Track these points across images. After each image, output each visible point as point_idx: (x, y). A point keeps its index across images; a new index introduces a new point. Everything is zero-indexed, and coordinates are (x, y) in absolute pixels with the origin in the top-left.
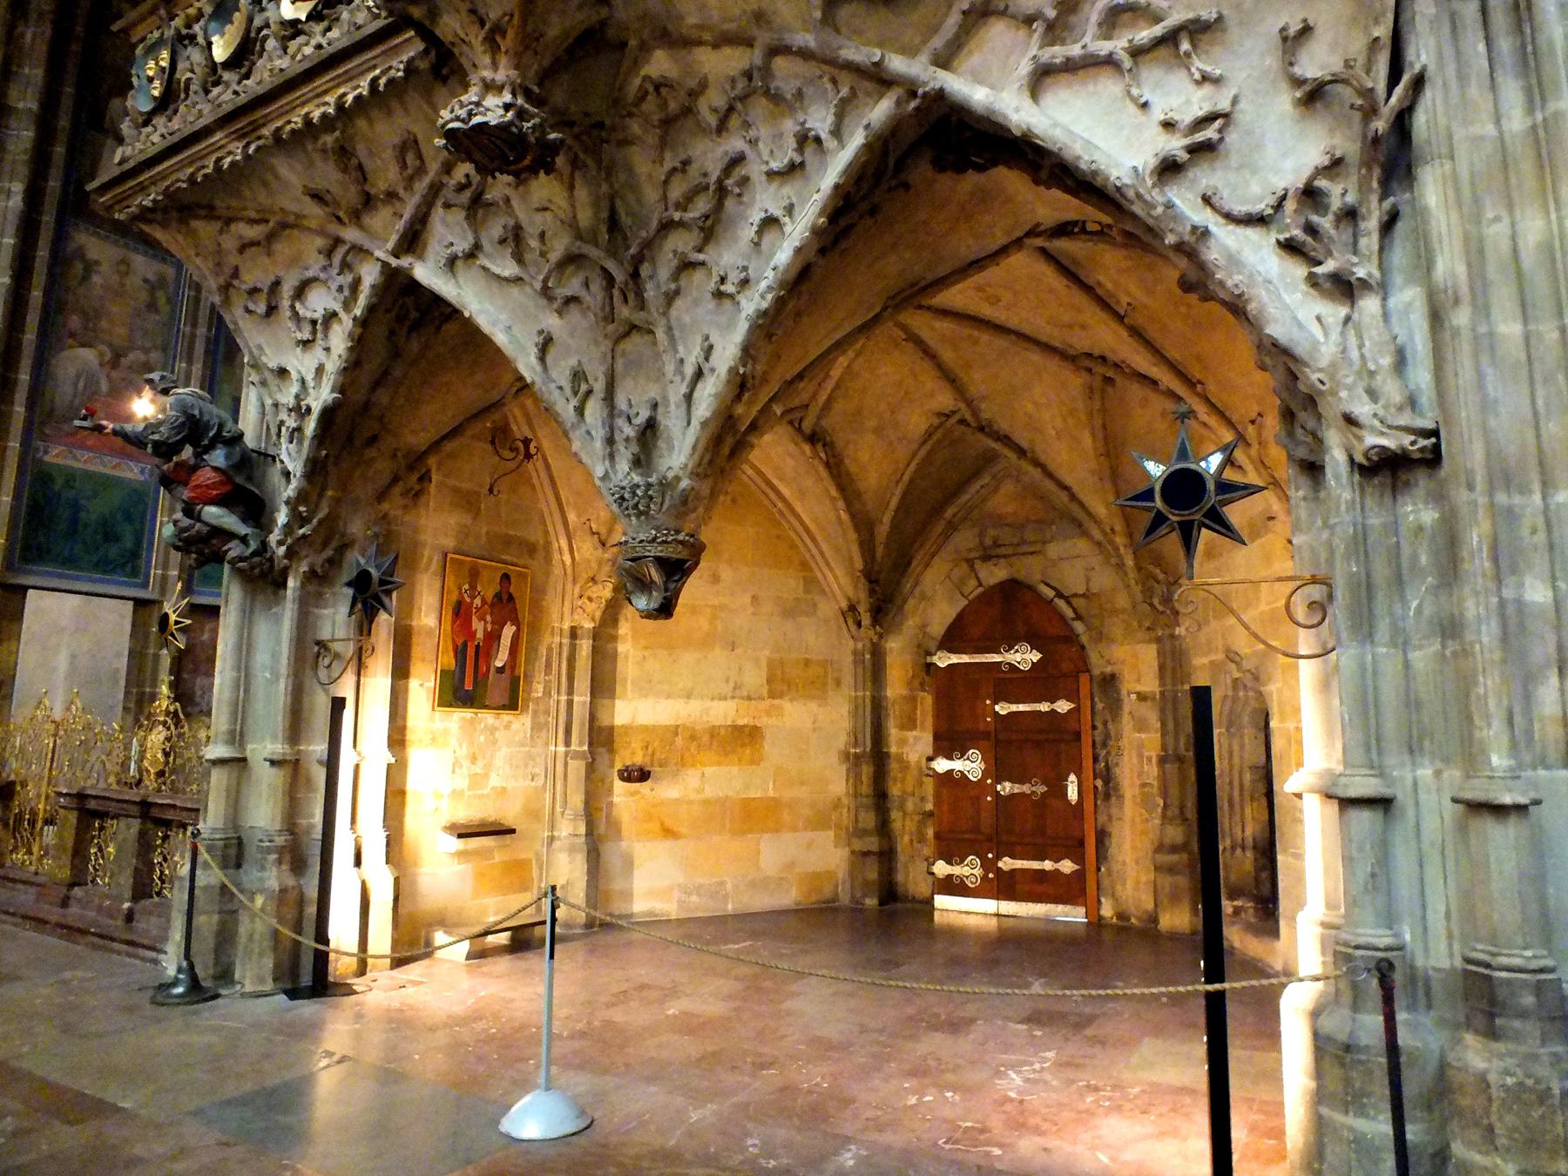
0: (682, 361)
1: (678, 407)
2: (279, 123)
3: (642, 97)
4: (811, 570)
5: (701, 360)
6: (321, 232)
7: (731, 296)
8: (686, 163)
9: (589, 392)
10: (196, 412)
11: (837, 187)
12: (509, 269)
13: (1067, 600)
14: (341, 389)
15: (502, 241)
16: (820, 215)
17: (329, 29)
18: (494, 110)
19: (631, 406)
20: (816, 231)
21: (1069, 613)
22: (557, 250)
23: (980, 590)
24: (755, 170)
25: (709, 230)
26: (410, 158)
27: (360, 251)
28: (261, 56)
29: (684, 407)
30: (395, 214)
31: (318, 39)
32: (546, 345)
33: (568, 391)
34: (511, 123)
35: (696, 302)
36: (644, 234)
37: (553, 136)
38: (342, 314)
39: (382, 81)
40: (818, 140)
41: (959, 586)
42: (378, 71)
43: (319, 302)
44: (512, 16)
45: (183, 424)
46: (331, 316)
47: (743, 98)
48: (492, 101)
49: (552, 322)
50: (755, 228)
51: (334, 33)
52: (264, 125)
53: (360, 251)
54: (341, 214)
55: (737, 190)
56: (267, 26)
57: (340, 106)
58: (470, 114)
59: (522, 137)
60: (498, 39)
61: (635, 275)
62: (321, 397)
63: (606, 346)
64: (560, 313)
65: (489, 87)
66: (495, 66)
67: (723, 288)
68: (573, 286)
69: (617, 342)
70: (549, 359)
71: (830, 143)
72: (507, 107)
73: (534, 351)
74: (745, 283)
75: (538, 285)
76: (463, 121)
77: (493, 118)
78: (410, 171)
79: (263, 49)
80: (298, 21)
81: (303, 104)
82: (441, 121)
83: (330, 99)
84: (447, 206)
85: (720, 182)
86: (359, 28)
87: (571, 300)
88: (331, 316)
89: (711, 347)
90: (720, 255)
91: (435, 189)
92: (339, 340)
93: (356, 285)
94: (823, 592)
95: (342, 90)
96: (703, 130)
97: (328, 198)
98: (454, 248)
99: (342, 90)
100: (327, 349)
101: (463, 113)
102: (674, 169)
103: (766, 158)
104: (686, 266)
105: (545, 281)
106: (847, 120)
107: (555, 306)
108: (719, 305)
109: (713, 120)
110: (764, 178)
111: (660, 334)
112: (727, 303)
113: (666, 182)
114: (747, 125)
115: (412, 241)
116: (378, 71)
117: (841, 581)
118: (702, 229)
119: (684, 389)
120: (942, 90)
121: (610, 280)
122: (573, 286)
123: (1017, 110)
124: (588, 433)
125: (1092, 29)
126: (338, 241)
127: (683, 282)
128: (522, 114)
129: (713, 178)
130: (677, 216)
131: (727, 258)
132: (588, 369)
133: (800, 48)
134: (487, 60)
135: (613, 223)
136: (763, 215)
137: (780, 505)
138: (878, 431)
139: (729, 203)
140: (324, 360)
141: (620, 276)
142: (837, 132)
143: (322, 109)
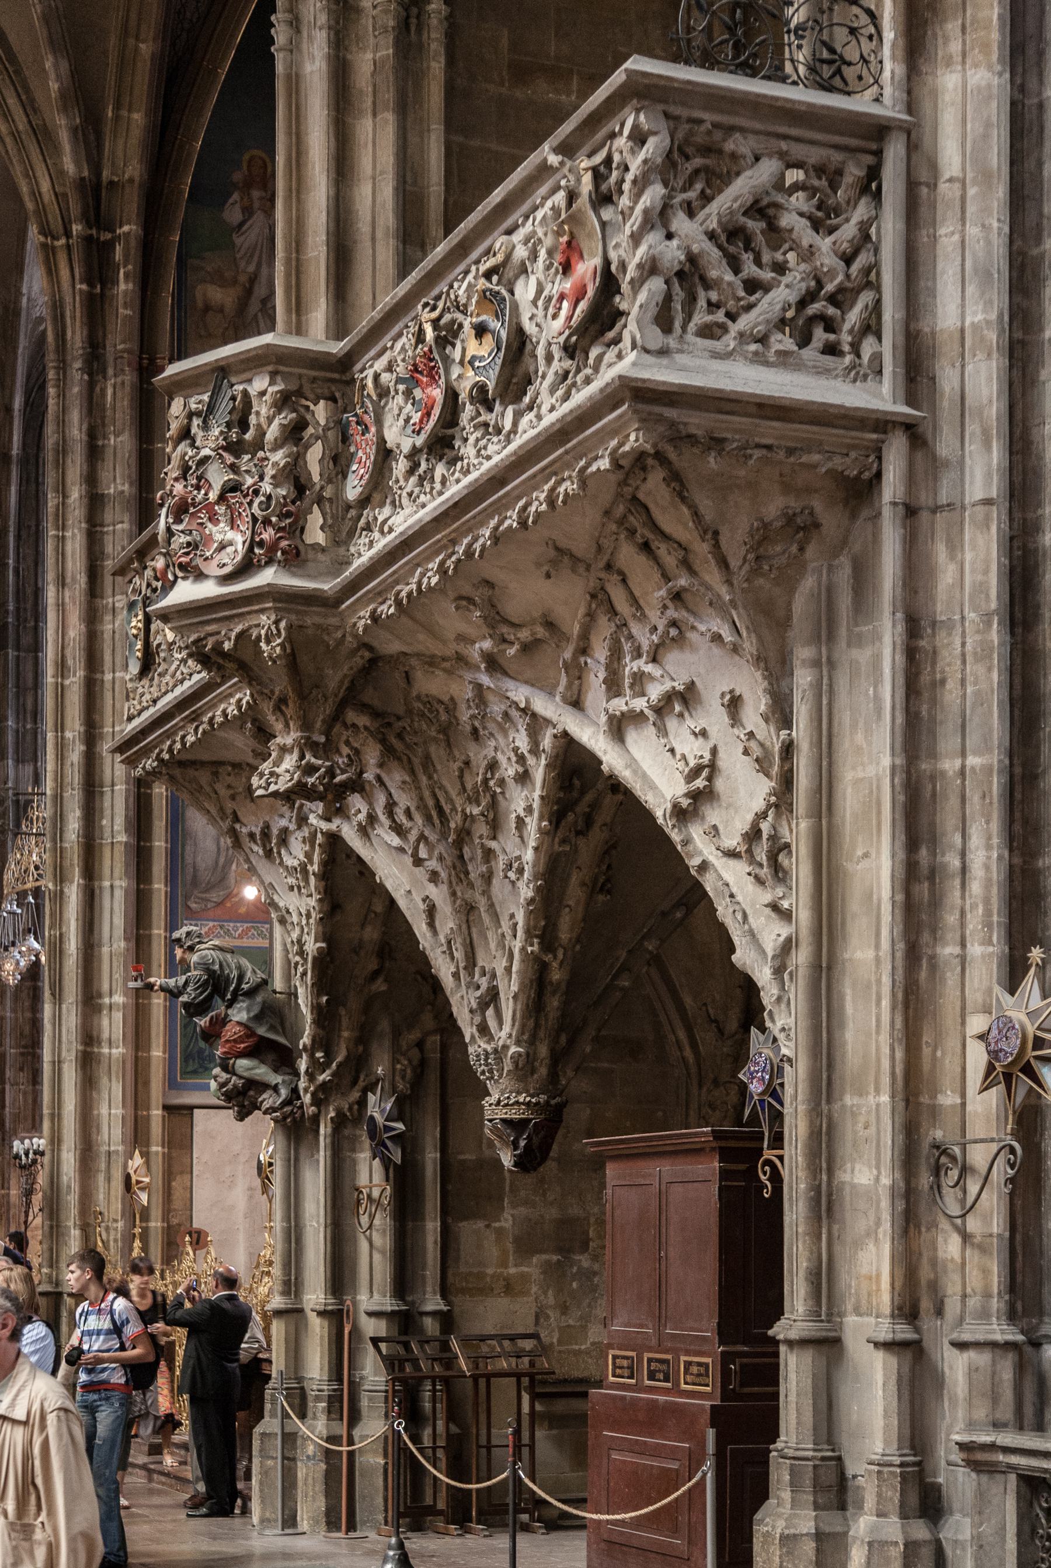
10: (217, 967)
11: (542, 798)
16: (541, 818)
32: (431, 911)
45: (206, 982)
62: (312, 946)
71: (531, 761)
85: (486, 781)
120: (565, 734)
123: (605, 753)
125: (628, 691)
139: (500, 798)
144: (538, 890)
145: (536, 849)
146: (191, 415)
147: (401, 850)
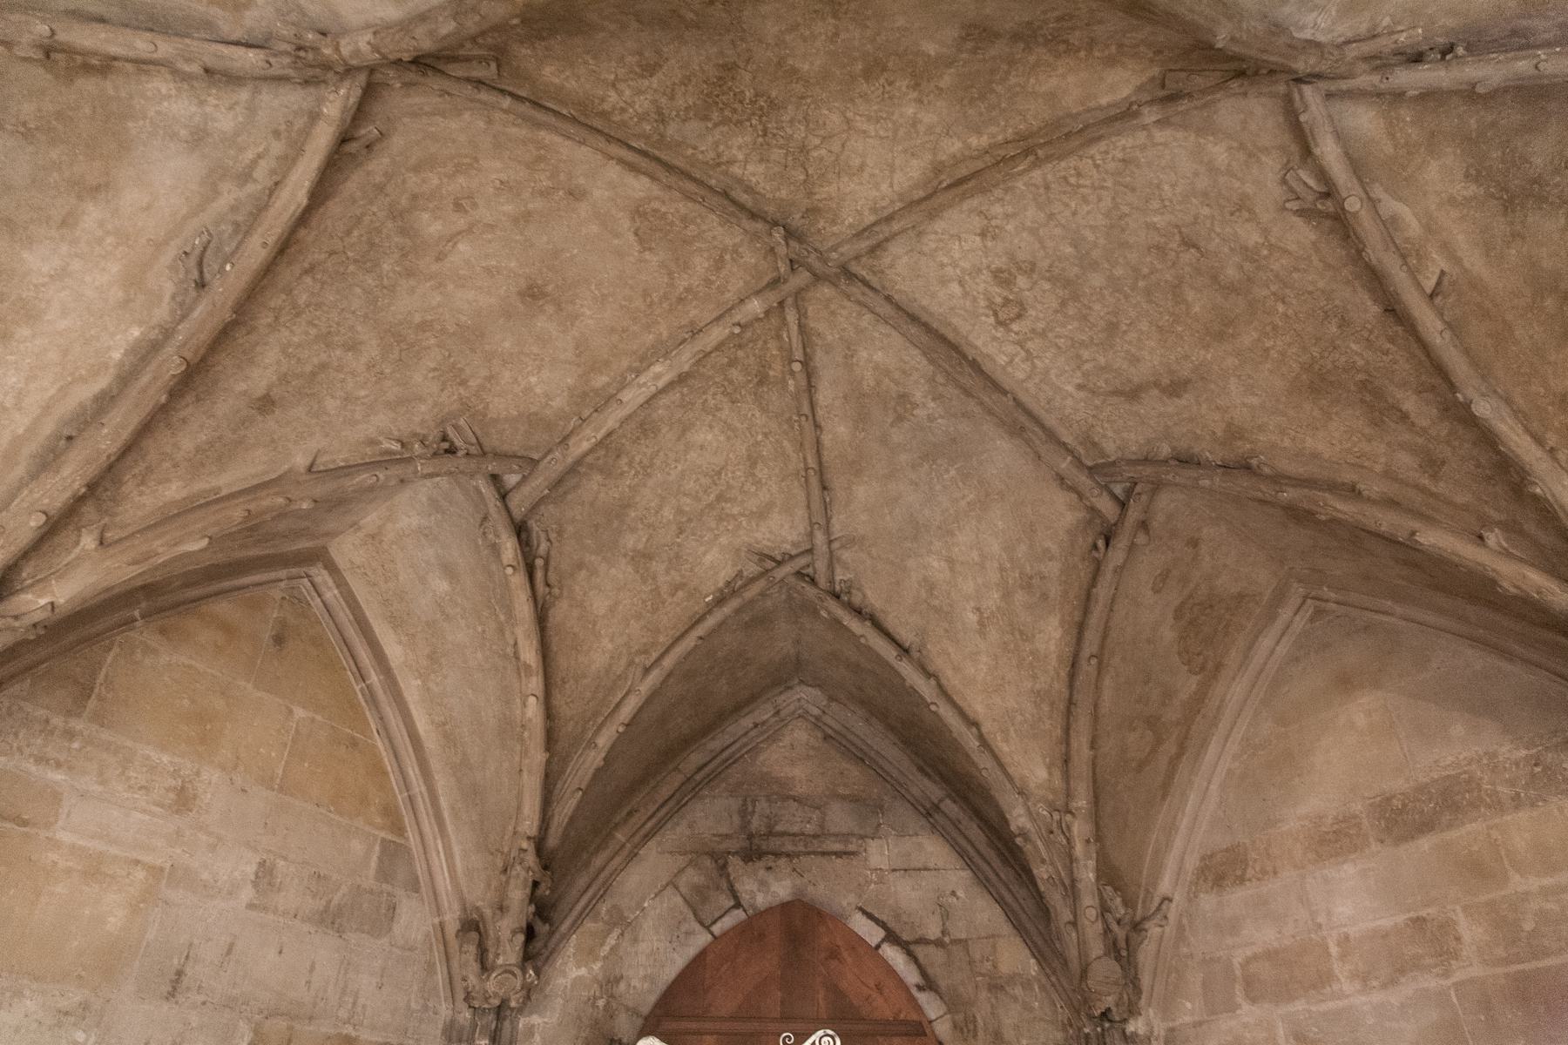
4: (399, 829)
13: (906, 947)
21: (911, 976)
23: (739, 915)
41: (697, 904)
94: (414, 886)
117: (461, 865)
137: (374, 678)
138: (642, 558)
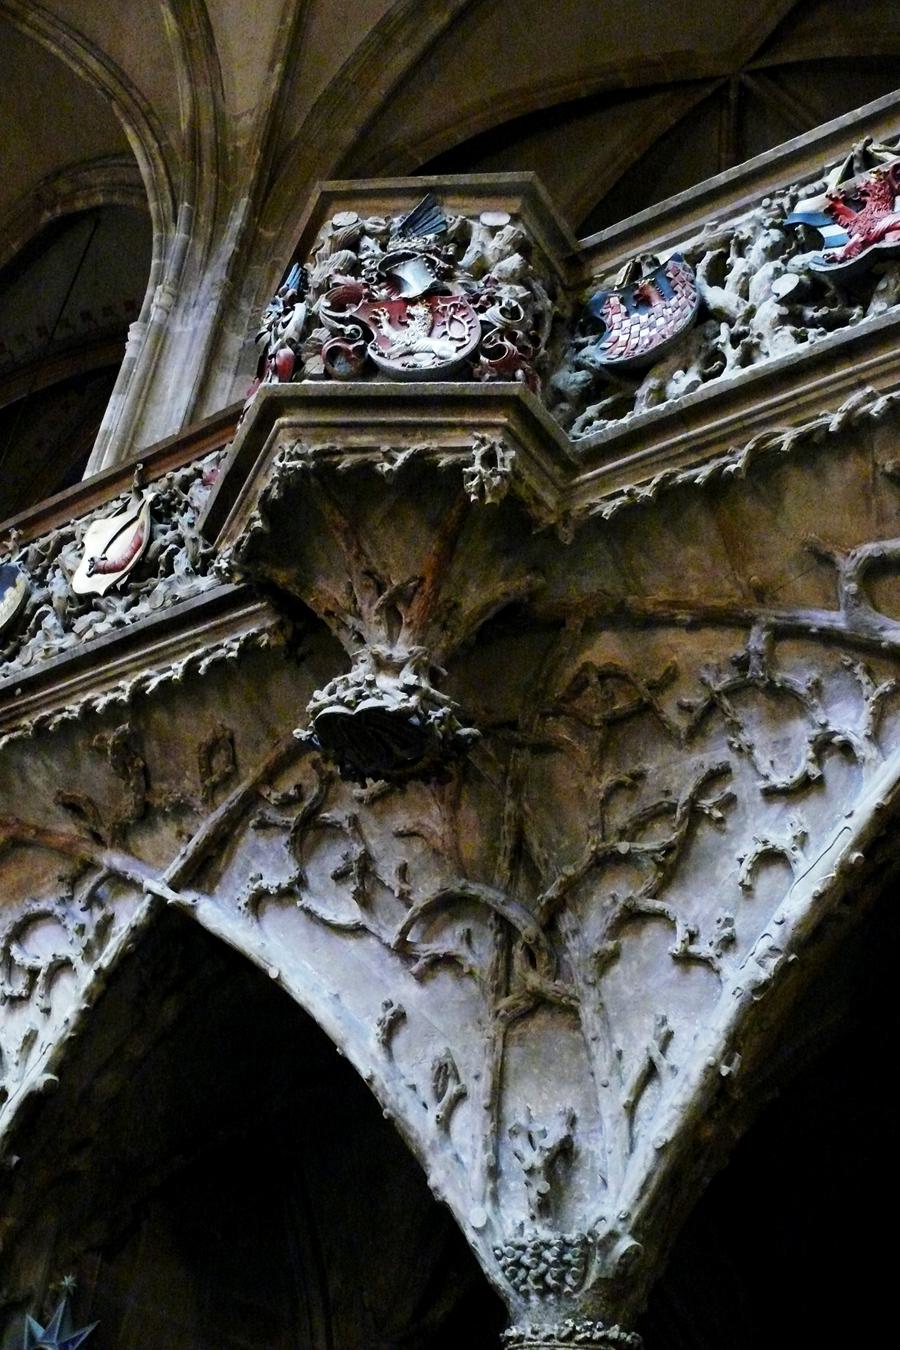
0: (620, 1054)
1: (616, 1123)
2: (46, 713)
3: (579, 685)
5: (656, 1054)
6: (65, 852)
7: (706, 962)
8: (639, 776)
9: (461, 1097)
11: (879, 811)
12: (347, 912)
14: (58, 1066)
15: (340, 877)
16: (853, 848)
17: (135, 603)
18: (391, 694)
19: (530, 1118)
20: (846, 871)
22: (425, 892)
24: (744, 786)
25: (673, 866)
26: (219, 763)
27: (121, 882)
28: (33, 635)
29: (625, 1123)
30: (180, 834)
31: (120, 614)
32: (394, 1024)
33: (426, 1093)
34: (413, 712)
35: (646, 970)
36: (570, 871)
37: (466, 731)
38: (78, 962)
39: (206, 661)
40: (846, 748)
42: (199, 652)
43: (42, 948)
44: (422, 580)
46: (62, 966)
47: (731, 692)
48: (385, 682)
49: (407, 991)
50: (747, 865)
51: (143, 608)
52: (26, 713)
53: (121, 882)
54: (102, 831)
55: (718, 814)
56: (48, 601)
57: (138, 691)
58: (359, 696)
59: (426, 730)
60: (401, 608)
61: (550, 926)
63: (493, 1028)
64: (421, 978)
65: (382, 664)
66: (392, 640)
67: (693, 949)
68: (448, 942)
69: (511, 1024)
70: (398, 1044)
72: (409, 690)
73: (374, 1032)
74: (729, 943)
75: (392, 938)
76: (348, 705)
77: (394, 702)
78: (215, 778)
79: (38, 627)
80: (95, 595)
81: (85, 690)
82: (312, 705)
83: (126, 684)
84: (263, 825)
85: (692, 802)
86: (181, 600)
87: (449, 961)
88: (62, 966)
89: (669, 1035)
90: (688, 903)
91: (251, 799)
92: (69, 999)
93: (104, 928)
95: (145, 673)
96: (666, 733)
97: (88, 809)
98: (264, 883)
99: (145, 673)
100: (47, 1011)
101: (349, 695)
102: (619, 785)
103: (764, 772)
104: (632, 918)
105: (404, 932)
106: (888, 722)
107: (415, 968)
108: (687, 971)
109: (682, 723)
110: (759, 798)
111: (587, 1012)
112: (699, 972)
113: (605, 803)
114: (735, 727)
115: (200, 872)
116: (199, 652)
118: (660, 865)
119: (625, 1097)
121: (507, 931)
122: (448, 942)
124: (457, 1158)
126: (89, 866)
127: (625, 941)
128: (428, 700)
129: (684, 796)
130: (624, 847)
131: (698, 907)
132: (460, 1059)
133: (822, 630)
134: (382, 632)
135: (520, 854)
136: (760, 848)
139: (705, 833)
140: (38, 1025)
141: (528, 928)
142: (875, 736)
143: (111, 696)
144: (784, 970)
145: (819, 899)
146: (364, 232)
147: (358, 931)
